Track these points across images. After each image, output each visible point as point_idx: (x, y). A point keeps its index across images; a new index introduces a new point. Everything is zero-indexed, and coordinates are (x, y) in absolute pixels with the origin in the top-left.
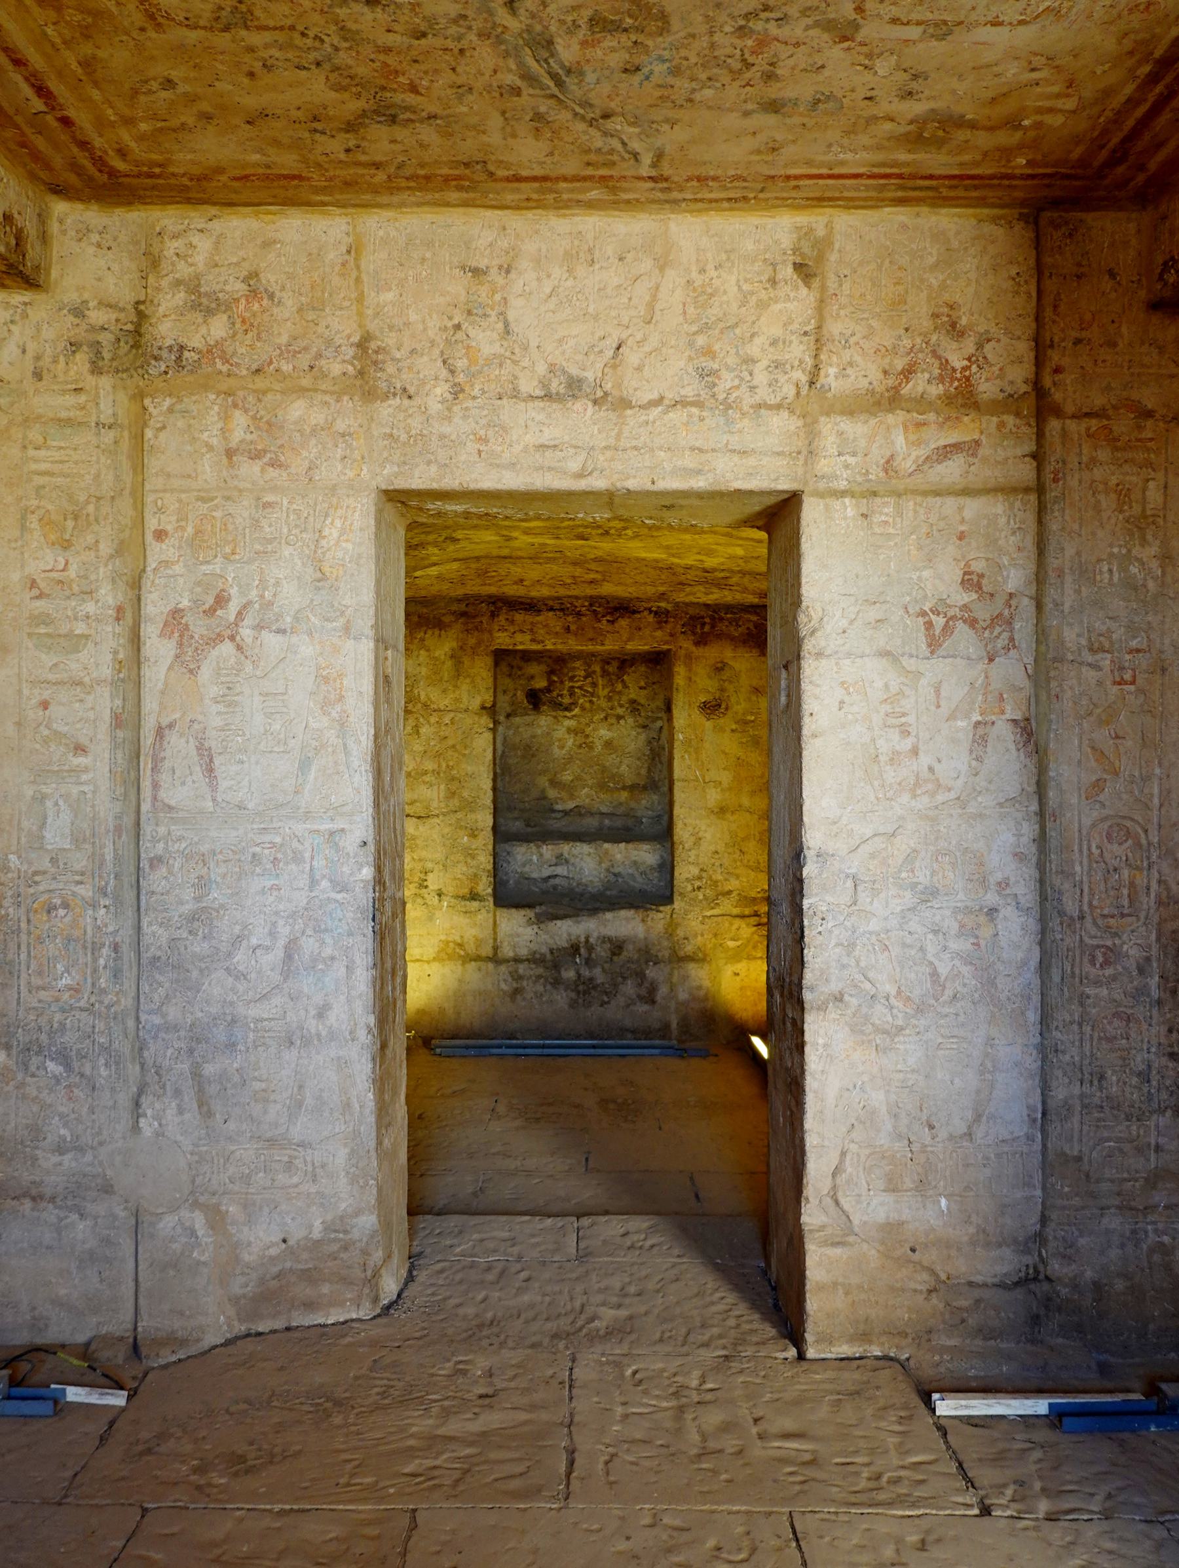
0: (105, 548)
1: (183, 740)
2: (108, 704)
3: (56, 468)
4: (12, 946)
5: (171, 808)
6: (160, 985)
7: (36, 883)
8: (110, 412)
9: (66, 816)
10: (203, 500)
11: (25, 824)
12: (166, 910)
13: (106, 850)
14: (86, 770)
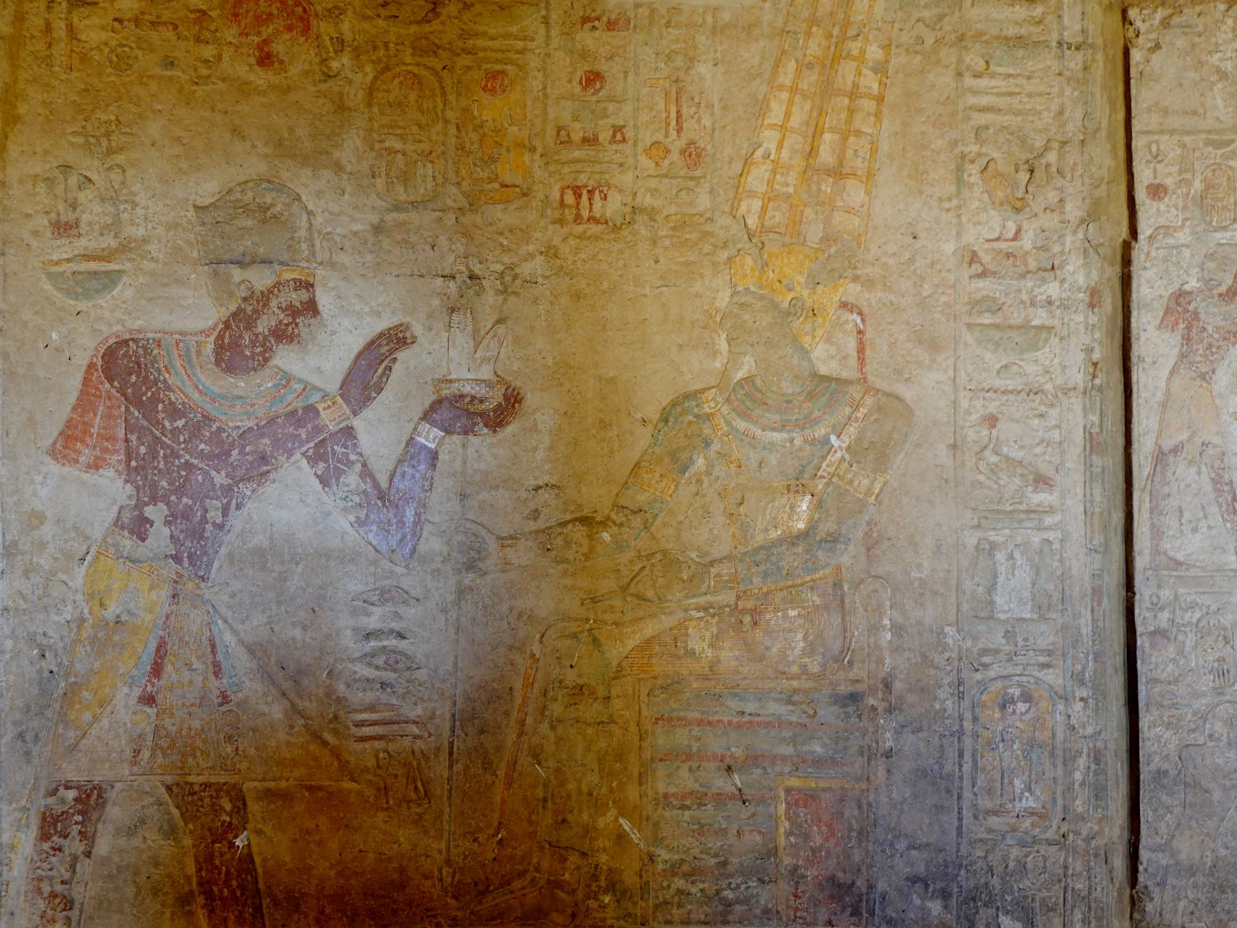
0: (1073, 210)
1: (1193, 470)
2: (1080, 420)
3: (1002, 102)
4: (952, 754)
5: (1179, 563)
6: (1169, 810)
7: (985, 666)
8: (1078, 27)
9: (1024, 575)
10: (1217, 145)
11: (968, 585)
12: (1175, 706)
13: (1082, 621)
14: (1051, 510)
